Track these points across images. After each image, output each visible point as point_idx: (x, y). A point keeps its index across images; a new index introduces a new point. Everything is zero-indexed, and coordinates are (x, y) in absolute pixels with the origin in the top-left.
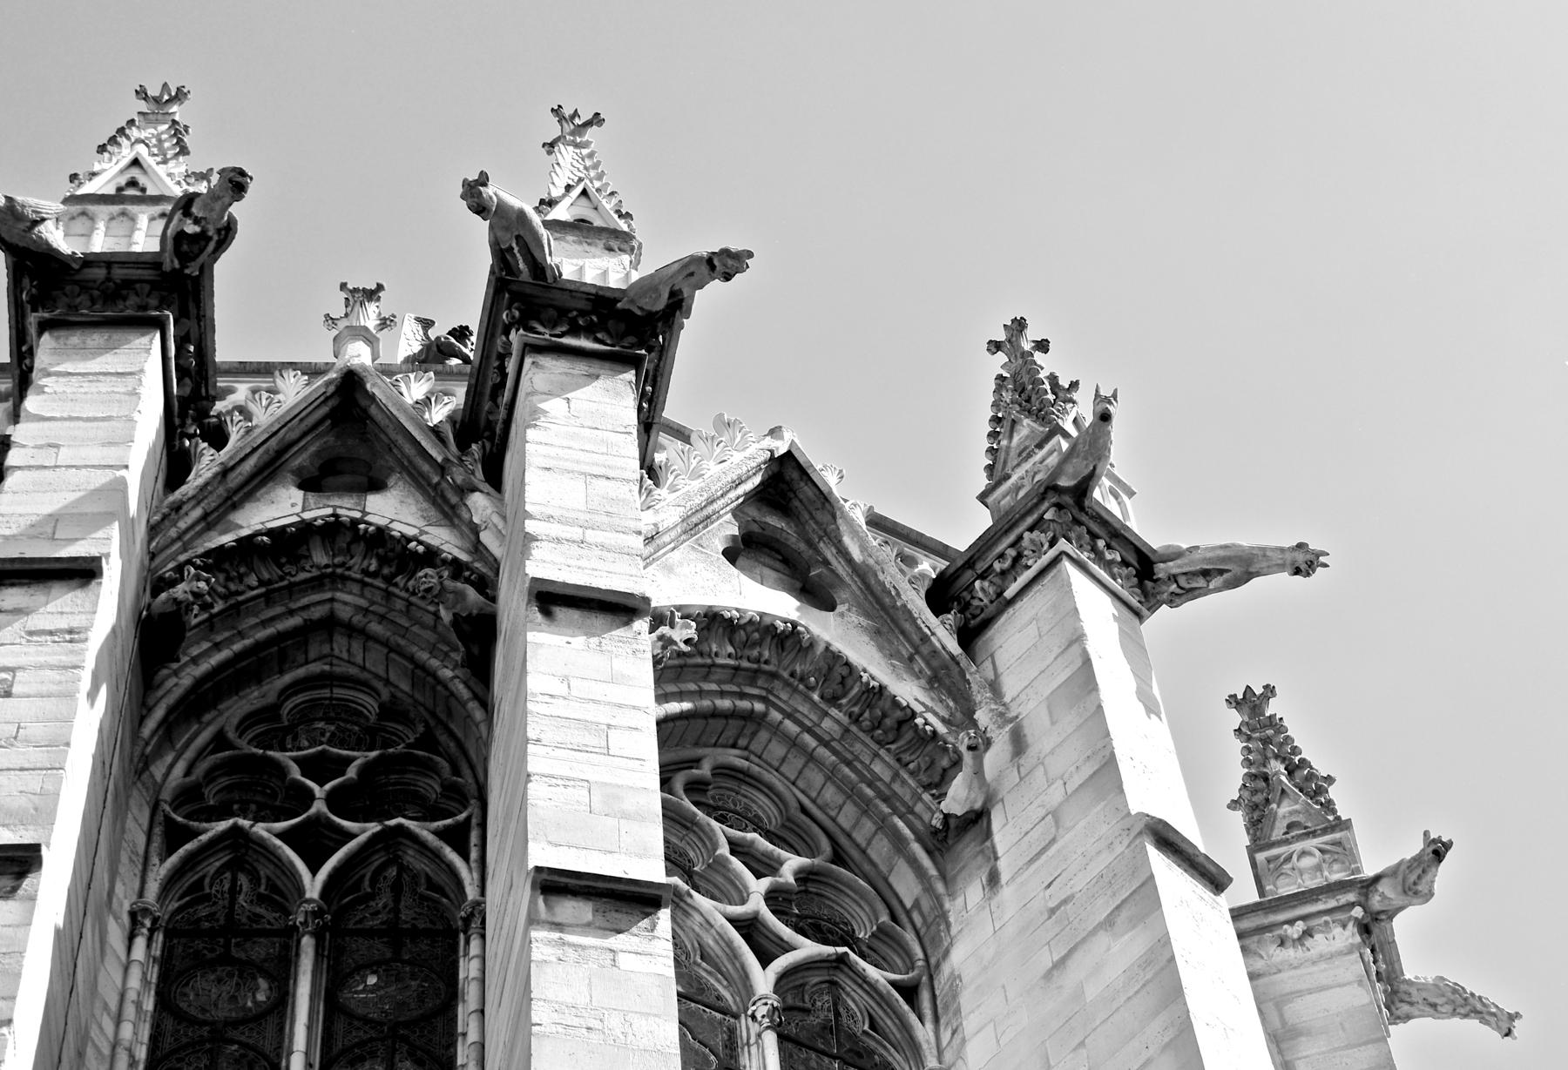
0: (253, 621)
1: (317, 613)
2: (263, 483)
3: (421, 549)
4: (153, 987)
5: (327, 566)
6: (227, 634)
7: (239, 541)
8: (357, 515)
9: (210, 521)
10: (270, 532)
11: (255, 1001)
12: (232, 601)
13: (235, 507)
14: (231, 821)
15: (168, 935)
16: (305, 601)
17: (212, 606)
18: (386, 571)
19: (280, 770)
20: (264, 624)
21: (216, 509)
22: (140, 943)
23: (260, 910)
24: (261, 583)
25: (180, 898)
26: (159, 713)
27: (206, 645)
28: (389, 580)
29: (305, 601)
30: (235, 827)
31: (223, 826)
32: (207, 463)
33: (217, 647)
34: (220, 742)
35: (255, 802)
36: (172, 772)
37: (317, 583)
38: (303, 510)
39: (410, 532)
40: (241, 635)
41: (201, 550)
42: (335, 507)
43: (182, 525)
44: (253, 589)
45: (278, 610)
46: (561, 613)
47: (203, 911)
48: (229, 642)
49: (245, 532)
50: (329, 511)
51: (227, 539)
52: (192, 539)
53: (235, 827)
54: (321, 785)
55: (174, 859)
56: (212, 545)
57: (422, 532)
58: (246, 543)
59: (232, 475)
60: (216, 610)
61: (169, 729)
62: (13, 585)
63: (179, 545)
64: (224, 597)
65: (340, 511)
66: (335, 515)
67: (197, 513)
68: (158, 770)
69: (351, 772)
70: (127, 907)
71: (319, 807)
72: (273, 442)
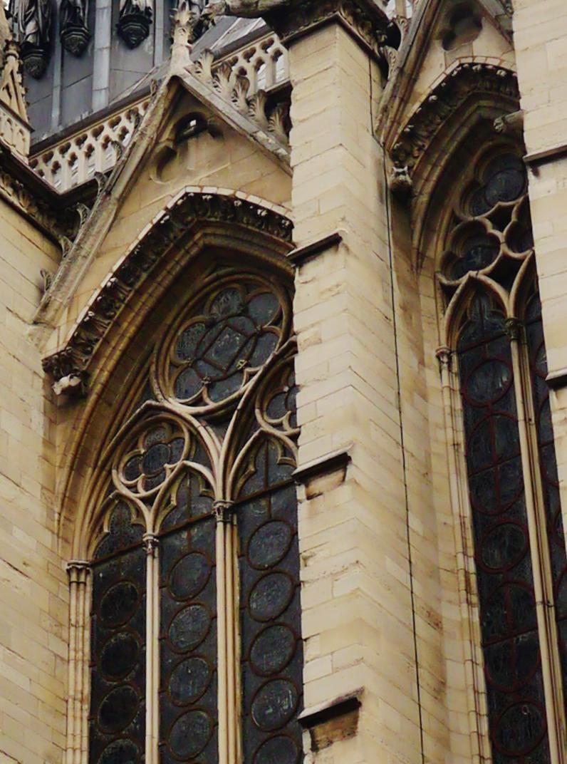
0: (447, 139)
1: (474, 118)
2: (425, 56)
3: (503, 73)
4: (458, 392)
5: (469, 92)
6: (437, 155)
7: (422, 105)
8: (470, 60)
9: (405, 101)
10: (434, 92)
11: (503, 384)
12: (432, 137)
13: (415, 80)
14: (467, 275)
15: (459, 353)
16: (467, 115)
17: (424, 146)
18: (494, 86)
19: (481, 226)
20: (452, 139)
21: (406, 92)
22: (445, 372)
23: (495, 320)
24: (441, 119)
25: (459, 329)
26: (418, 226)
27: (429, 168)
28: (498, 90)
29: (467, 115)
30: (471, 278)
31: (464, 280)
32: (395, 56)
33: (435, 166)
34: (455, 219)
35: (479, 246)
36: (437, 250)
37: (469, 102)
38: (446, 68)
39: (496, 63)
40: (444, 152)
41: (406, 121)
42: (459, 59)
43: (391, 115)
44: (439, 124)
45: (457, 126)
46: (544, 169)
47: (471, 330)
48: (439, 159)
49: (423, 98)
50: (457, 63)
51: (415, 108)
52: (400, 117)
53: (471, 278)
54: (502, 231)
55: (448, 311)
56: (410, 115)
57: (502, 61)
58: (425, 104)
59: (406, 69)
60: (426, 147)
61: (428, 229)
62: (309, 261)
63: (395, 124)
64: (428, 137)
65: (463, 61)
66: (461, 65)
67: (397, 101)
68: (430, 253)
69: (514, 218)
70: (434, 354)
71: (504, 248)
72: (421, 31)
